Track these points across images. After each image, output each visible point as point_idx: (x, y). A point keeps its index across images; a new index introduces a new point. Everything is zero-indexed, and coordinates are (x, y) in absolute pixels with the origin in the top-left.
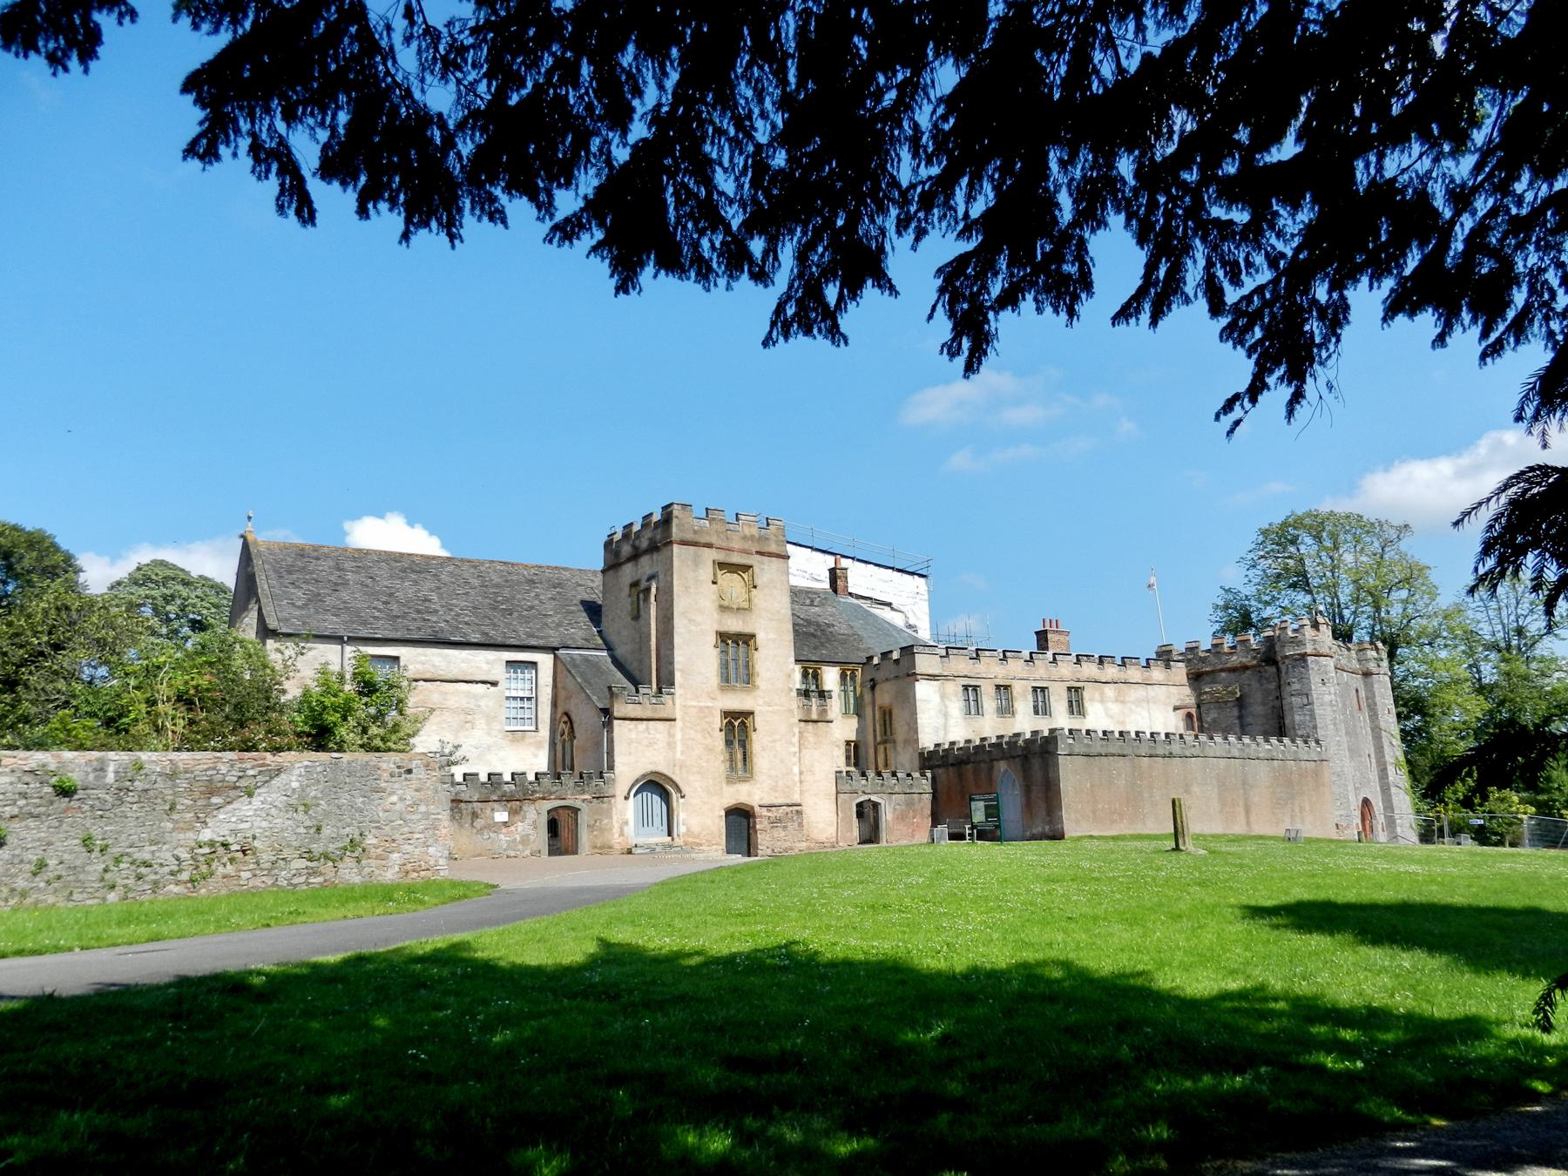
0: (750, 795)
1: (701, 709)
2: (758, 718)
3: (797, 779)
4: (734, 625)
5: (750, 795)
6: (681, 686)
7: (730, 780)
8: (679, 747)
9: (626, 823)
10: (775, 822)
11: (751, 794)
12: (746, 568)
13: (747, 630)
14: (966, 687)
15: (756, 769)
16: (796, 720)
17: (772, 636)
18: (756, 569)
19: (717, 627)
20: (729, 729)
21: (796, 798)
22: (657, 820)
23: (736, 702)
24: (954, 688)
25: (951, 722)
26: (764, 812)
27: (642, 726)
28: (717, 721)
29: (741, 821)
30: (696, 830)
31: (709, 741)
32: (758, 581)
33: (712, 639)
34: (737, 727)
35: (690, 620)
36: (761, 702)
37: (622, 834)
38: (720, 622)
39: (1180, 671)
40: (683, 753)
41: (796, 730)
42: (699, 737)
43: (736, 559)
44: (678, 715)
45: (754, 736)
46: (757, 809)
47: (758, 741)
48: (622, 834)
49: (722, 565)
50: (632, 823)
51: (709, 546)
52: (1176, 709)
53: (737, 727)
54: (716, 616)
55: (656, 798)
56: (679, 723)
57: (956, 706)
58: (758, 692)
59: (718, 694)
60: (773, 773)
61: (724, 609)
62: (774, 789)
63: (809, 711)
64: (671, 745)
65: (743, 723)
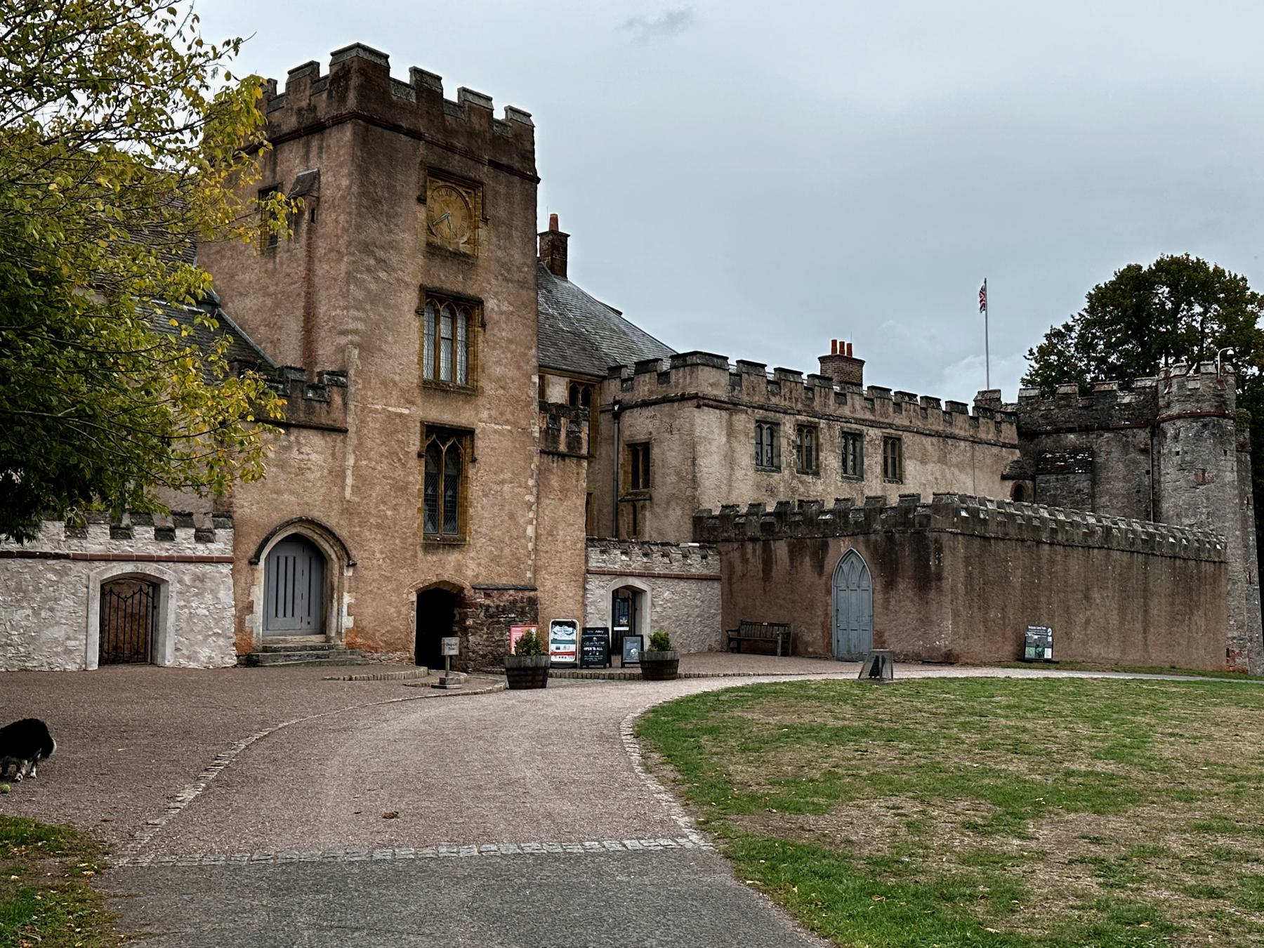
0: (459, 568)
1: (391, 417)
2: (479, 444)
3: (530, 546)
7: (430, 546)
8: (349, 481)
9: (250, 608)
11: (466, 568)
13: (471, 290)
14: (759, 424)
20: (430, 453)
22: (301, 605)
24: (744, 422)
25: (739, 474)
28: (415, 443)
30: (368, 623)
31: (400, 472)
34: (447, 452)
35: (380, 261)
36: (485, 414)
39: (1010, 433)
44: (351, 422)
45: (471, 472)
46: (469, 592)
50: (259, 608)
52: (1004, 478)
54: (420, 260)
55: (302, 565)
56: (352, 438)
57: (745, 453)
58: (482, 401)
61: (433, 251)
62: (495, 560)
63: (555, 439)
65: (454, 450)
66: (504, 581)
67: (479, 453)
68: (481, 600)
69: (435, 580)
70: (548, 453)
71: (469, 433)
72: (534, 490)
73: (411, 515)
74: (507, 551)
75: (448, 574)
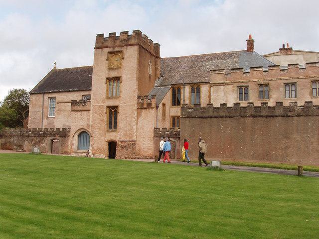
0: (116, 136)
1: (99, 106)
4: (113, 74)
5: (116, 136)
6: (93, 99)
10: (122, 147)
12: (120, 52)
13: (118, 75)
15: (118, 127)
16: (136, 108)
17: (129, 76)
18: (125, 52)
19: (107, 76)
21: (134, 138)
23: (111, 103)
26: (120, 144)
27: (79, 113)
28: (105, 110)
29: (112, 145)
32: (125, 56)
33: (105, 80)
37: (71, 148)
38: (109, 75)
40: (92, 122)
41: (136, 112)
42: (98, 116)
43: (117, 49)
44: (91, 108)
47: (120, 117)
48: (71, 148)
49: (110, 53)
51: (107, 47)
53: (113, 112)
54: (107, 72)
56: (91, 112)
58: (120, 98)
59: (106, 102)
60: (125, 129)
61: (110, 69)
62: (125, 135)
64: (88, 119)
66: (128, 139)
67: (120, 112)
68: (120, 144)
69: (110, 139)
70: (141, 108)
71: (117, 107)
72: (136, 118)
73: (104, 125)
74: (128, 133)
75: (113, 138)
